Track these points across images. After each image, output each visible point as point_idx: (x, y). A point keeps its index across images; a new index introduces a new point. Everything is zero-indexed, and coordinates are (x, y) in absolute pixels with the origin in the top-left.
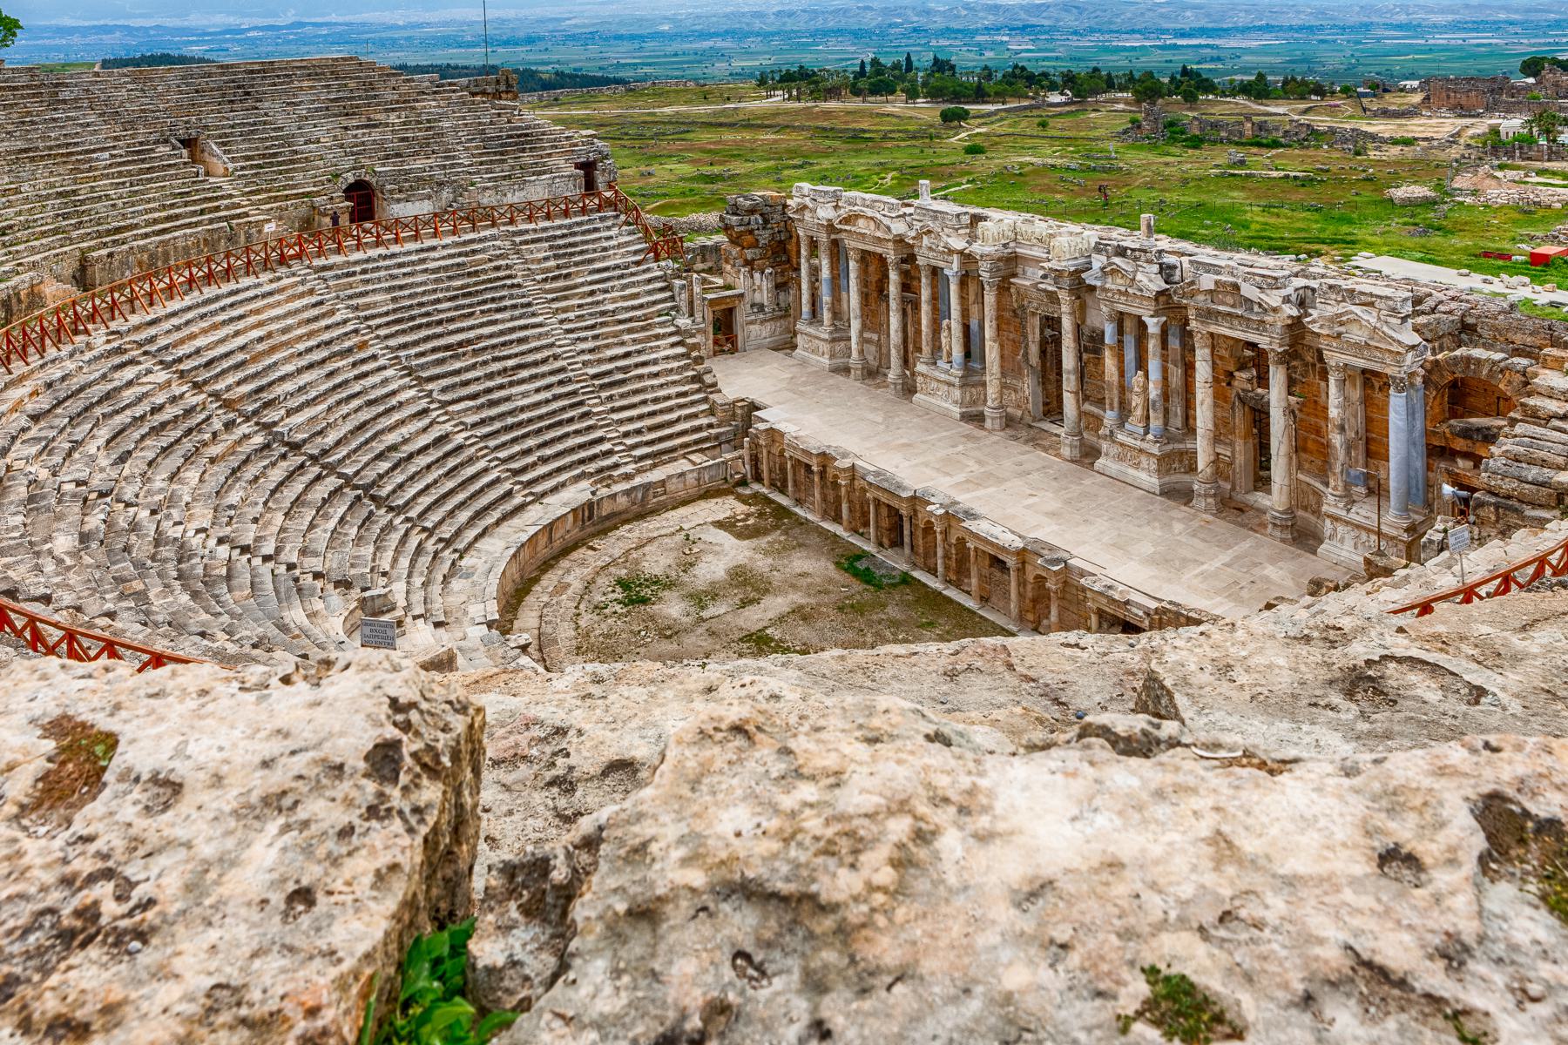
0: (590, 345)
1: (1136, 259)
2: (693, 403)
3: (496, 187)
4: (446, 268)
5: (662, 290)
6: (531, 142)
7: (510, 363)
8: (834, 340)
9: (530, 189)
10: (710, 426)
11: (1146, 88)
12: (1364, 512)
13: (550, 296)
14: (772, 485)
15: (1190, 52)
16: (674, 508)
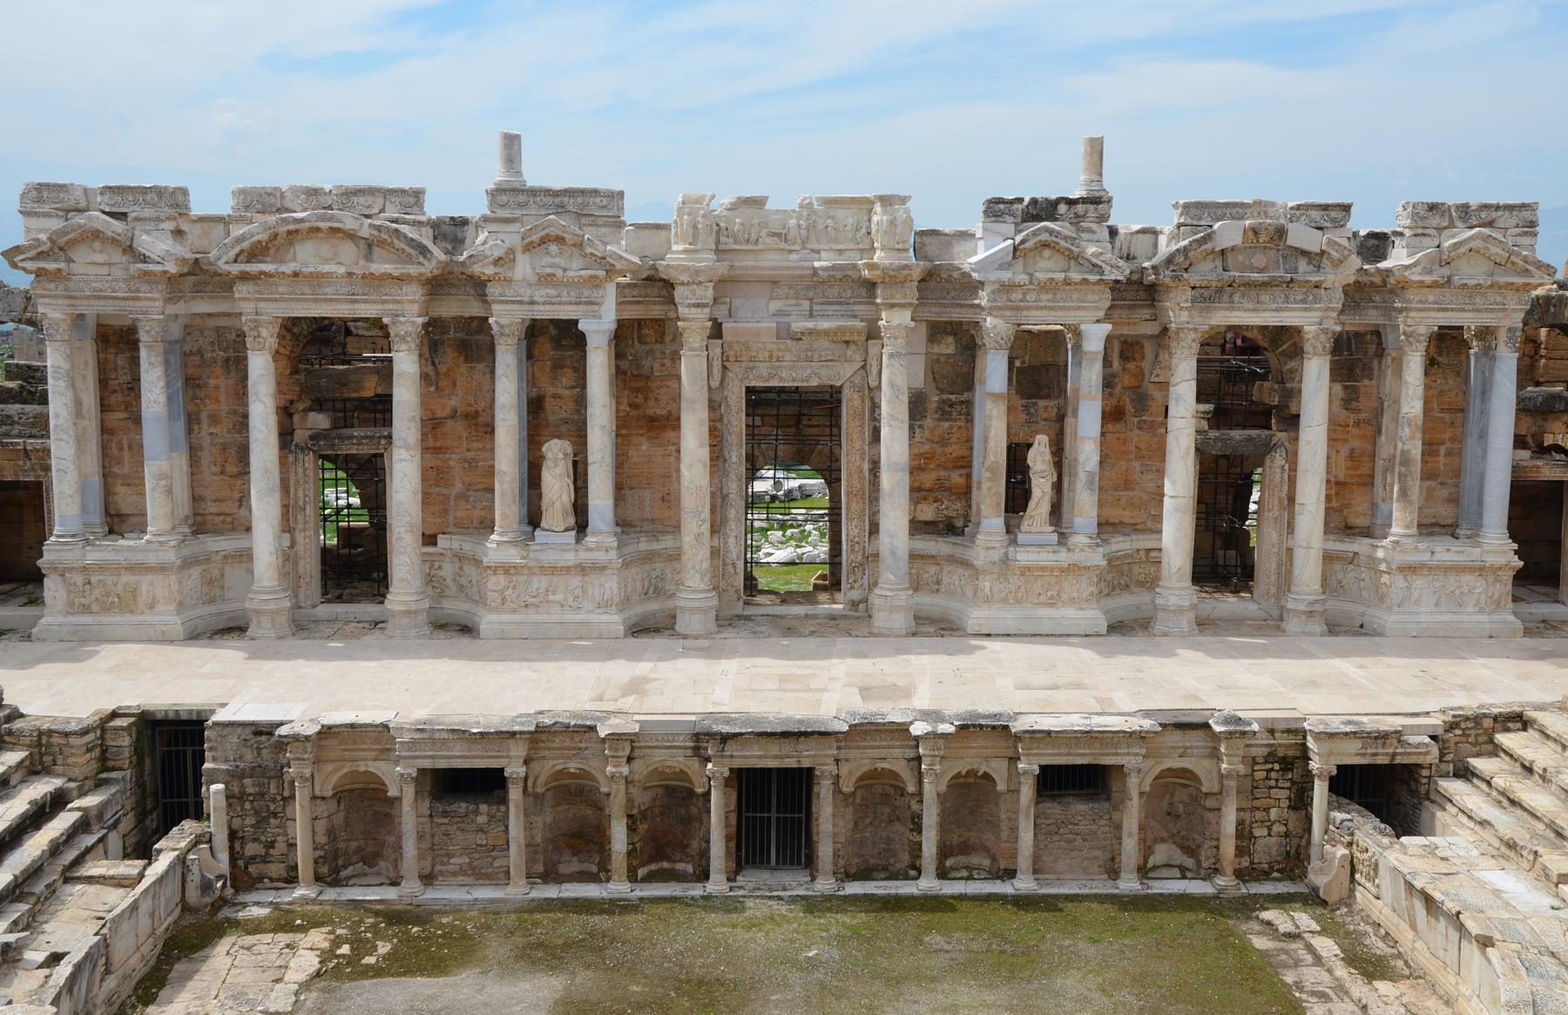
8: (187, 564)
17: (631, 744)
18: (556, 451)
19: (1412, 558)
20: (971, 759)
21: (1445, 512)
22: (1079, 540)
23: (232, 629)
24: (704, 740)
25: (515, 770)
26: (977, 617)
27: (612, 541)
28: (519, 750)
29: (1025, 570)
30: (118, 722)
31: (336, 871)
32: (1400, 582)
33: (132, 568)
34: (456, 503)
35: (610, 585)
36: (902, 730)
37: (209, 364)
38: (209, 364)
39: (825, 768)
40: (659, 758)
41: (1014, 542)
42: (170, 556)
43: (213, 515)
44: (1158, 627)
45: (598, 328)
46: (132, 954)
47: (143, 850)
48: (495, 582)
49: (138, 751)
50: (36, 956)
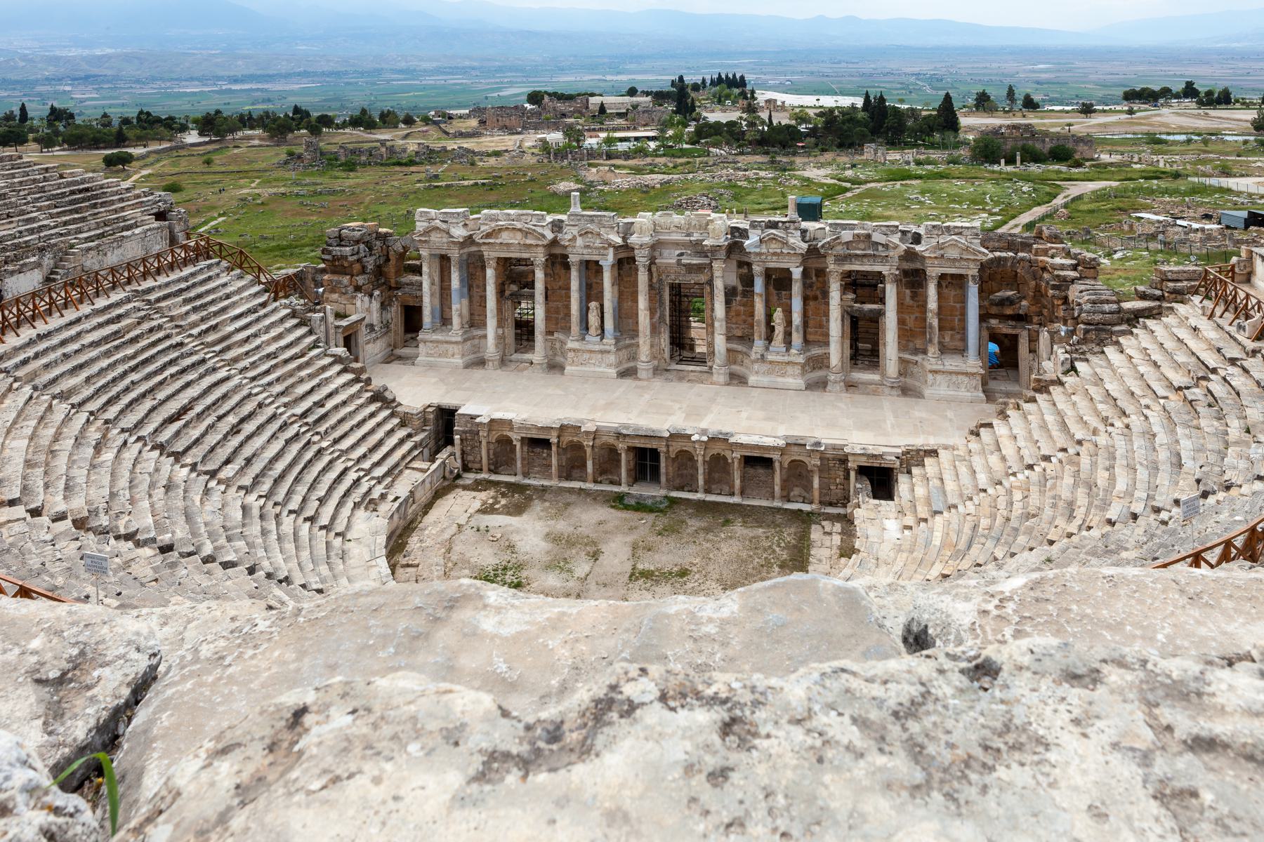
0: (278, 388)
1: (787, 228)
2: (385, 420)
3: (98, 247)
4: (105, 339)
5: (296, 326)
6: (96, 197)
7: (232, 419)
8: (465, 340)
9: (127, 245)
10: (409, 436)
11: (280, 126)
12: (952, 363)
13: (217, 348)
14: (490, 471)
15: (312, 98)
16: (426, 513)
17: (596, 434)
18: (593, 305)
19: (935, 367)
20: (716, 449)
21: (959, 344)
22: (793, 351)
23: (481, 363)
24: (619, 435)
25: (554, 440)
26: (752, 379)
27: (613, 342)
28: (555, 434)
29: (771, 362)
30: (430, 410)
31: (496, 468)
32: (930, 376)
33: (447, 342)
34: (558, 320)
35: (612, 358)
36: (689, 436)
37: (474, 266)
38: (474, 266)
39: (662, 449)
40: (604, 439)
41: (767, 349)
42: (459, 339)
43: (475, 321)
44: (829, 388)
45: (608, 261)
46: (423, 496)
47: (433, 460)
48: (570, 355)
49: (437, 418)
50: (391, 497)
